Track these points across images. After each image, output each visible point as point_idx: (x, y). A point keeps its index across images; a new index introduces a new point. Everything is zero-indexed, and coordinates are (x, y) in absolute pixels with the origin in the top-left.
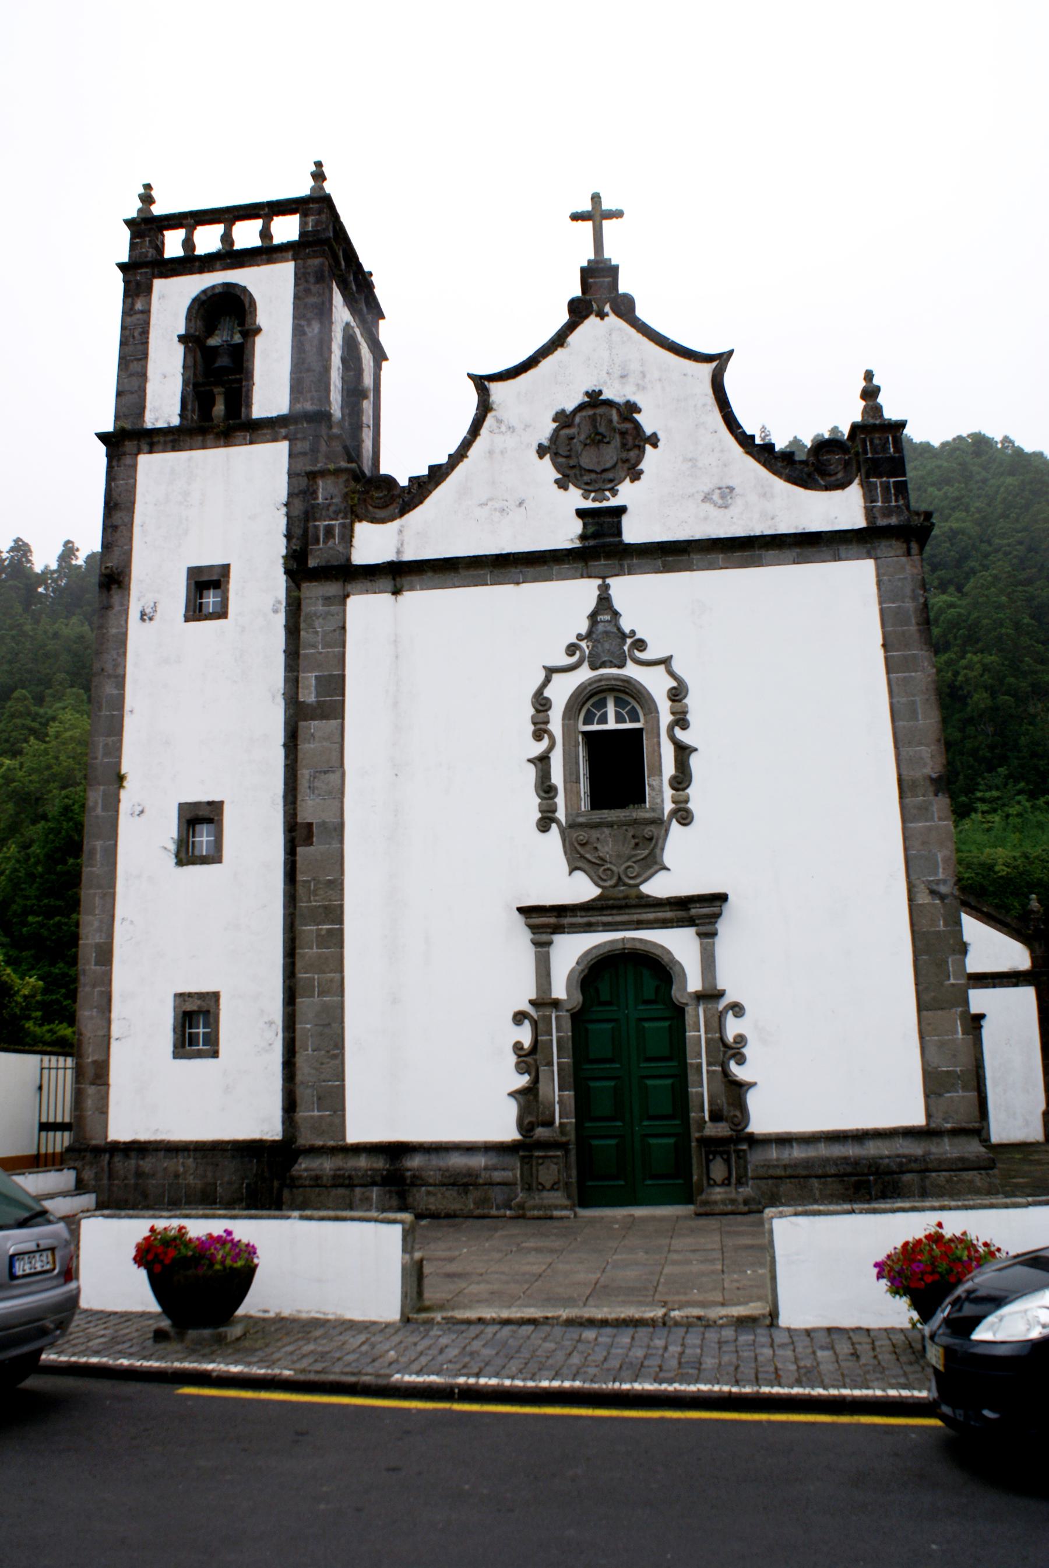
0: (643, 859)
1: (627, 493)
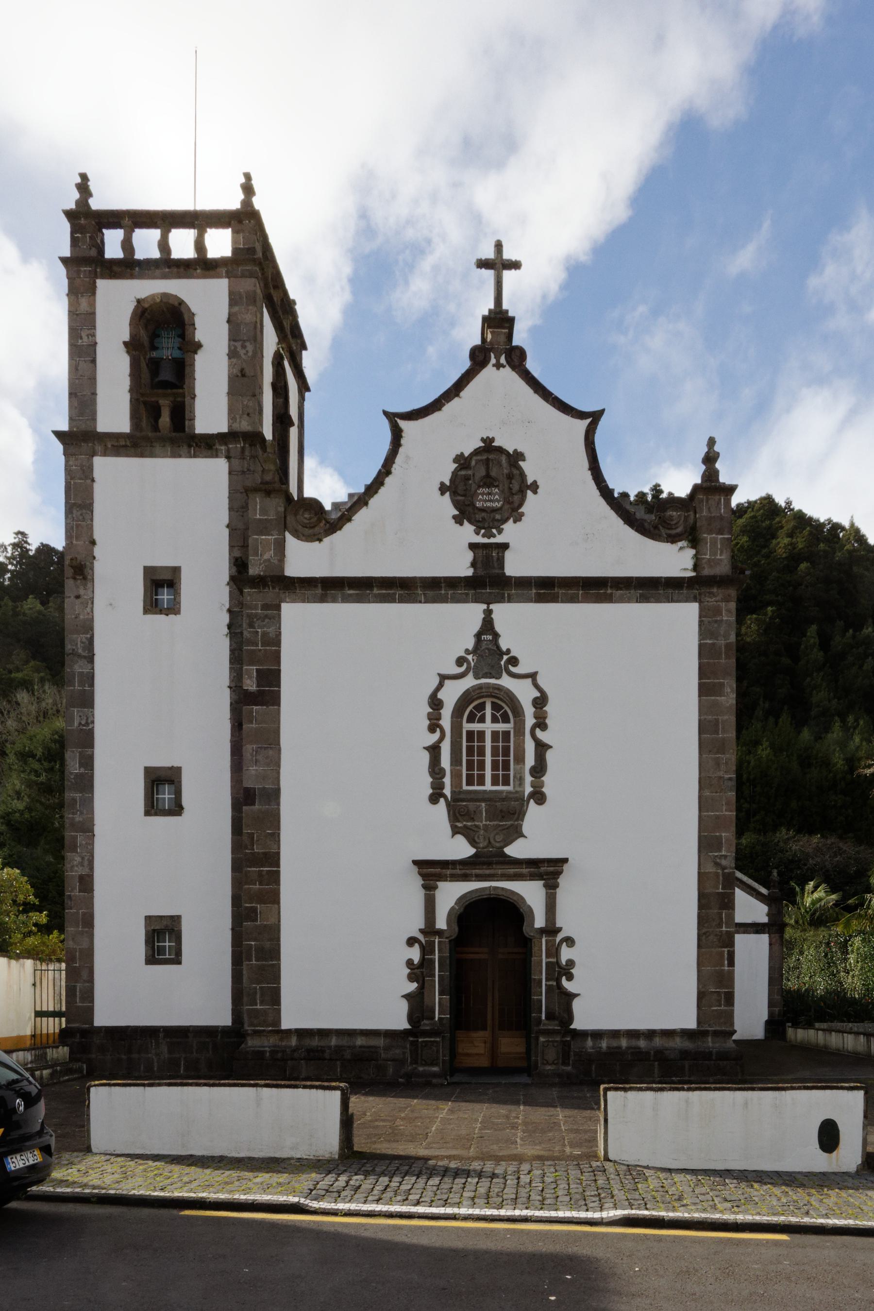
0: (507, 828)
1: (510, 532)
